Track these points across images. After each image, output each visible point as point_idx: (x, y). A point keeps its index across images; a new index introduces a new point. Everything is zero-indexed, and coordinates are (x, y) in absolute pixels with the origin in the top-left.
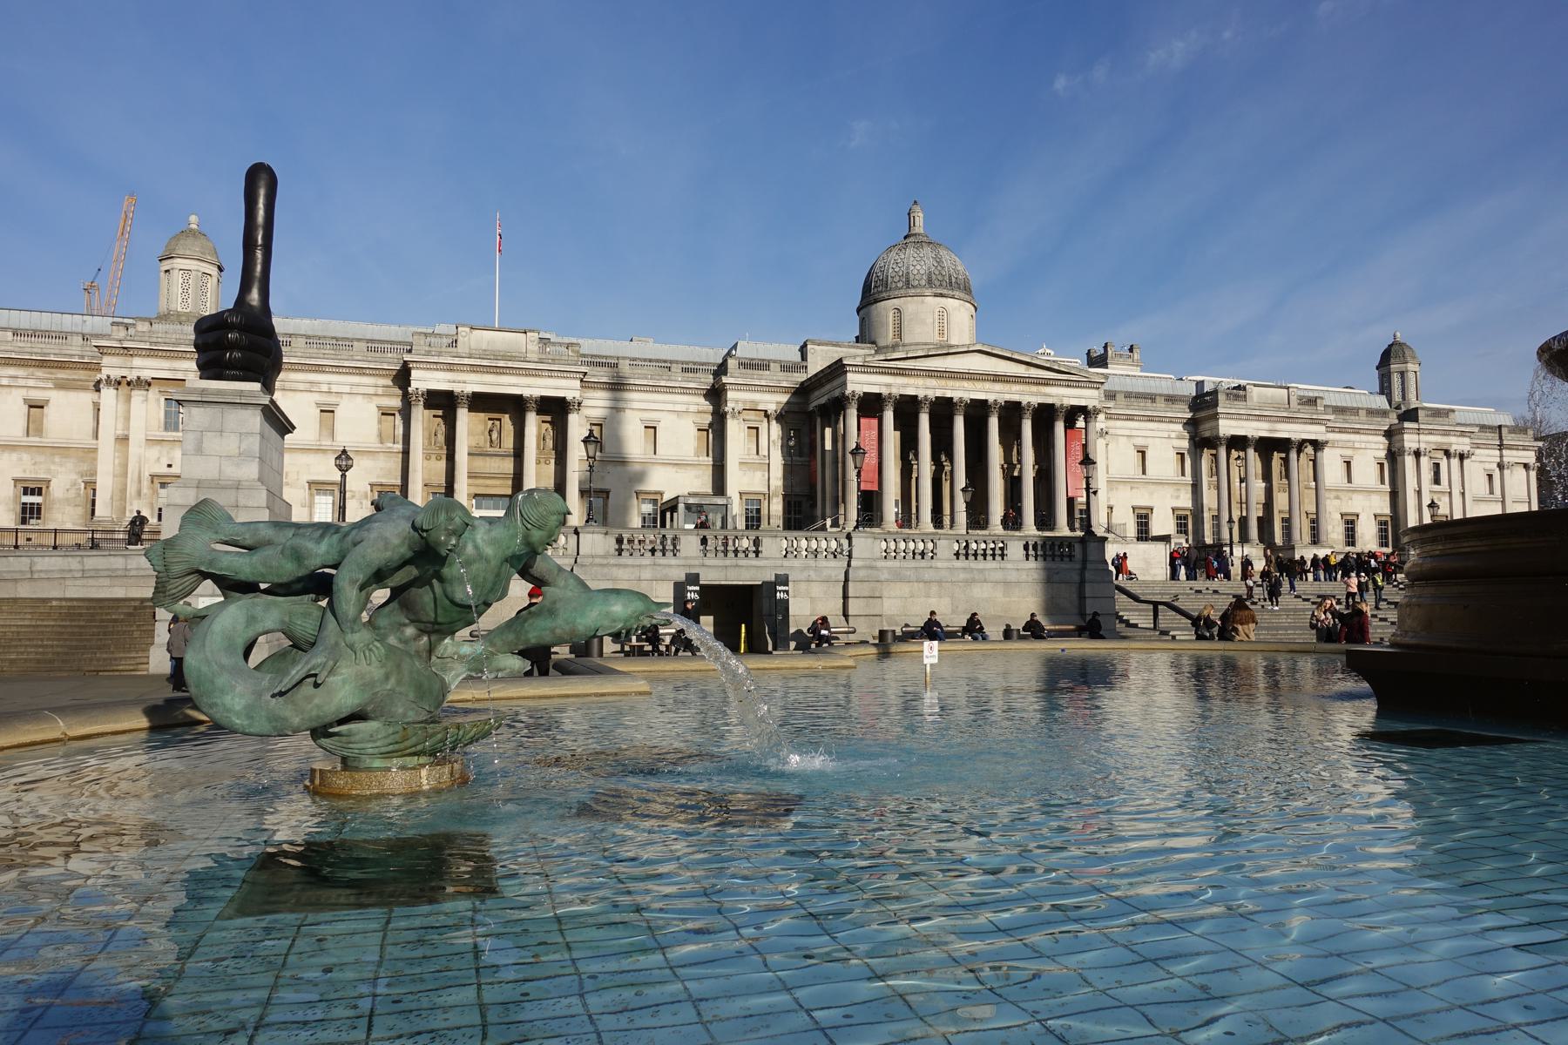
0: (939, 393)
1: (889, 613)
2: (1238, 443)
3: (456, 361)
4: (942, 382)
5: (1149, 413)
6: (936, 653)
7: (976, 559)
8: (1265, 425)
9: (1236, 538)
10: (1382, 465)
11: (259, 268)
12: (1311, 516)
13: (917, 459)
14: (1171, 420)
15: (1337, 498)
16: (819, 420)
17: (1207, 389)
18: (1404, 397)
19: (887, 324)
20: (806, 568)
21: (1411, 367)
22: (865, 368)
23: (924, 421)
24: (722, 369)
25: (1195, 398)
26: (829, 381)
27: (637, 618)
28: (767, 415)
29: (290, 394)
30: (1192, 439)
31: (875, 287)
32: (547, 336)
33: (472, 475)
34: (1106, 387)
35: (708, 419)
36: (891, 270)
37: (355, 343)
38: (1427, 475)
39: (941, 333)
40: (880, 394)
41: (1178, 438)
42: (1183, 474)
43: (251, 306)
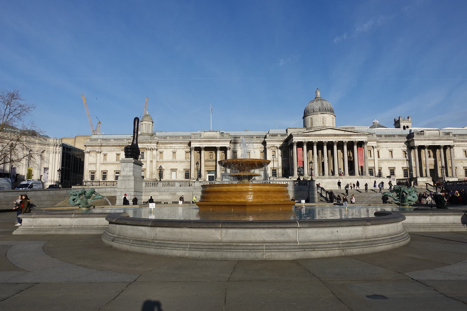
0: (319, 140)
3: (201, 140)
4: (320, 137)
5: (392, 140)
8: (431, 142)
11: (136, 137)
13: (324, 157)
14: (400, 142)
15: (462, 162)
17: (412, 132)
19: (309, 122)
22: (298, 135)
26: (291, 139)
28: (277, 148)
29: (167, 149)
30: (407, 147)
32: (223, 132)
33: (205, 166)
35: (263, 149)
37: (180, 137)
39: (323, 123)
41: (403, 147)
43: (134, 143)
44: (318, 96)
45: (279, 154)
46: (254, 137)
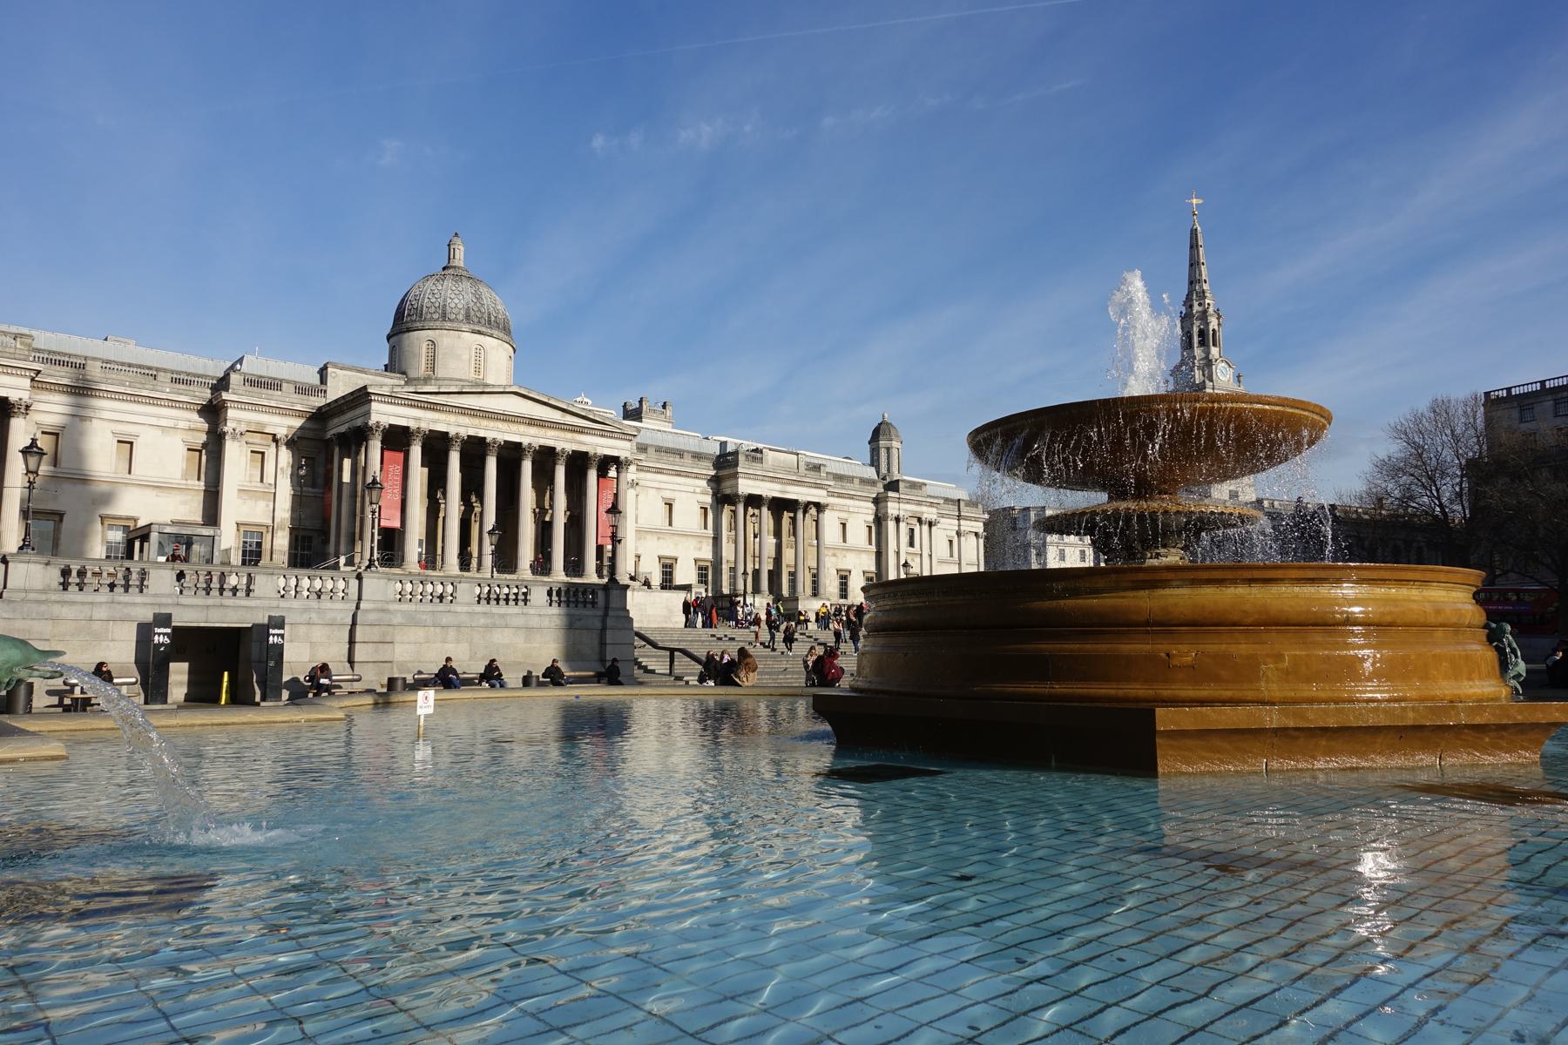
0: (472, 432)
1: (401, 659)
2: (754, 501)
4: (476, 421)
6: (431, 702)
7: (498, 604)
8: (778, 487)
9: (749, 589)
10: (870, 527)
12: (812, 571)
13: (445, 498)
14: (697, 476)
15: (834, 555)
16: (337, 450)
17: (730, 449)
18: (889, 470)
20: (306, 610)
21: (895, 444)
22: (392, 399)
23: (454, 459)
24: (222, 384)
25: (719, 457)
26: (351, 409)
27: (10, 671)
28: (275, 439)
30: (714, 495)
31: (409, 315)
34: (638, 439)
35: (203, 438)
36: (426, 300)
38: (904, 539)
39: (477, 371)
40: (408, 428)
42: (706, 528)
44: (456, 263)
45: (282, 469)
46: (162, 374)
